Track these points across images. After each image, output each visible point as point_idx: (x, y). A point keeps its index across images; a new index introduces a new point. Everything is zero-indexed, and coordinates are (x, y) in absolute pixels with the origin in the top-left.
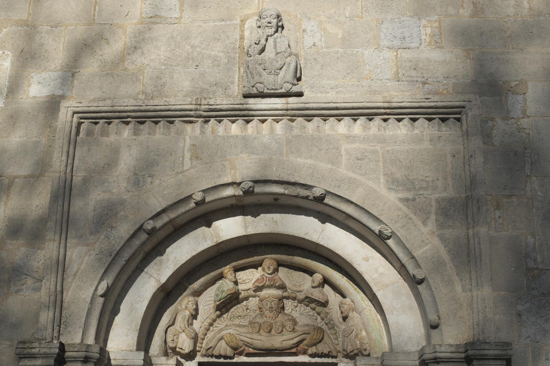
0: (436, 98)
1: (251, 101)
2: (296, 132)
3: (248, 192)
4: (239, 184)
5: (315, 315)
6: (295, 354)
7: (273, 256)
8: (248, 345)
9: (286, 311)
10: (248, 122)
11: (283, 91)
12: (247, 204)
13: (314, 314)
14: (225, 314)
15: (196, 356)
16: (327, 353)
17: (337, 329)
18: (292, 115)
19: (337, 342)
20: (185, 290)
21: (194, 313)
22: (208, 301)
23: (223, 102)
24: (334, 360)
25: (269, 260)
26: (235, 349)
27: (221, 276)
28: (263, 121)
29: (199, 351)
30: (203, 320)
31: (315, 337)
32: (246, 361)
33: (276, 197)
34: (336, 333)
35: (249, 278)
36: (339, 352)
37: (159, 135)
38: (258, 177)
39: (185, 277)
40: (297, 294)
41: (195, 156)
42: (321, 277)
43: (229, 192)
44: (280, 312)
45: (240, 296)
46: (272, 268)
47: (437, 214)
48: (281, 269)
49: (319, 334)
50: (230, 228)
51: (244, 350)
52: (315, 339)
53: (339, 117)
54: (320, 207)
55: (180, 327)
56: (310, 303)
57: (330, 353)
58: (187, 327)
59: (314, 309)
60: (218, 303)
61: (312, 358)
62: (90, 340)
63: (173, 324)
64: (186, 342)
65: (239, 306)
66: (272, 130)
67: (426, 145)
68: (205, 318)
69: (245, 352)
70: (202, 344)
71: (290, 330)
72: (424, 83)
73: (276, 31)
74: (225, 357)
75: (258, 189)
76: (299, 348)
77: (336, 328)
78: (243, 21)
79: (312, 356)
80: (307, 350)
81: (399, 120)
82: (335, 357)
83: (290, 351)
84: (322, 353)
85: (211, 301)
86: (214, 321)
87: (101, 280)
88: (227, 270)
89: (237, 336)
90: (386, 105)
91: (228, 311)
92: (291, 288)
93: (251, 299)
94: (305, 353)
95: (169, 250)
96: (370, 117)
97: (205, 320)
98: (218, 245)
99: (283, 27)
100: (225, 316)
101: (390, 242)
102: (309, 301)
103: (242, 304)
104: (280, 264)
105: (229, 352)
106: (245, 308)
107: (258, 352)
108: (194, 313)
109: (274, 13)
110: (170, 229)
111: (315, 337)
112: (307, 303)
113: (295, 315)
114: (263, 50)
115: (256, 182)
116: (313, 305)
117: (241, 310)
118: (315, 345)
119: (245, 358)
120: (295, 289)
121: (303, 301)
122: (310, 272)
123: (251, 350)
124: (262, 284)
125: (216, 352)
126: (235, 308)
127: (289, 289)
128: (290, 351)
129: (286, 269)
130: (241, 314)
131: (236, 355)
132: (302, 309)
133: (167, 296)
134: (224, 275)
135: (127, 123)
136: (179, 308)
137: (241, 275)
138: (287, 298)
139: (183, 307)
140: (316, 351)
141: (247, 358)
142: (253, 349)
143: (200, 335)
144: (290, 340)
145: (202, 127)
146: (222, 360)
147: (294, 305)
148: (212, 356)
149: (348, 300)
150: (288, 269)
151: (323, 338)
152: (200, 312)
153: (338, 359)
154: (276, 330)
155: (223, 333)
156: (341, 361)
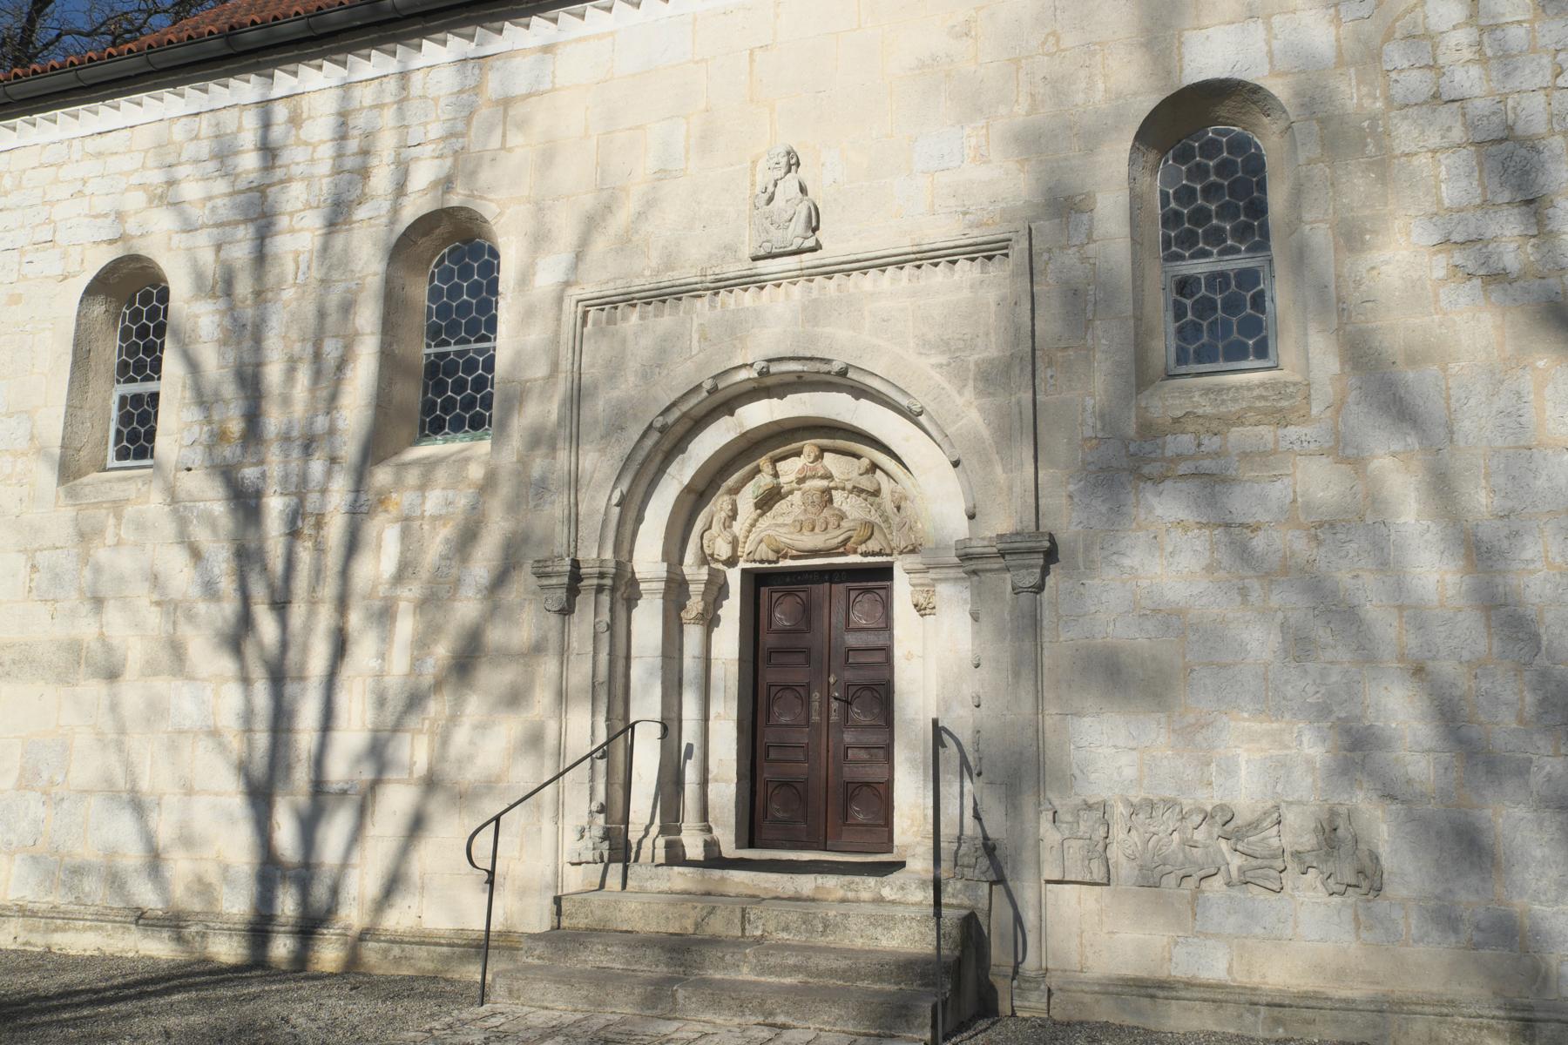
0: (975, 232)
1: (760, 263)
2: (815, 294)
3: (763, 373)
4: (751, 365)
10: (762, 288)
11: (793, 248)
12: (767, 386)
18: (810, 275)
22: (747, 500)
23: (732, 270)
24: (889, 559)
25: (809, 446)
26: (777, 552)
27: (758, 471)
28: (779, 286)
33: (799, 375)
35: (790, 469)
37: (665, 320)
38: (772, 356)
41: (704, 338)
43: (743, 375)
47: (975, 380)
50: (758, 414)
53: (864, 270)
54: (840, 381)
62: (608, 554)
63: (710, 527)
66: (787, 295)
67: (966, 293)
72: (965, 213)
73: (789, 171)
75: (774, 368)
78: (754, 163)
79: (865, 554)
81: (936, 265)
87: (614, 487)
88: (764, 462)
90: (915, 249)
91: (771, 508)
94: (855, 552)
95: (691, 447)
96: (900, 265)
98: (743, 435)
99: (798, 164)
101: (922, 419)
105: (772, 556)
109: (783, 150)
110: (688, 423)
113: (845, 508)
114: (771, 199)
115: (770, 361)
122: (858, 457)
133: (698, 495)
135: (634, 306)
137: (781, 466)
138: (836, 488)
143: (741, 539)
145: (711, 301)
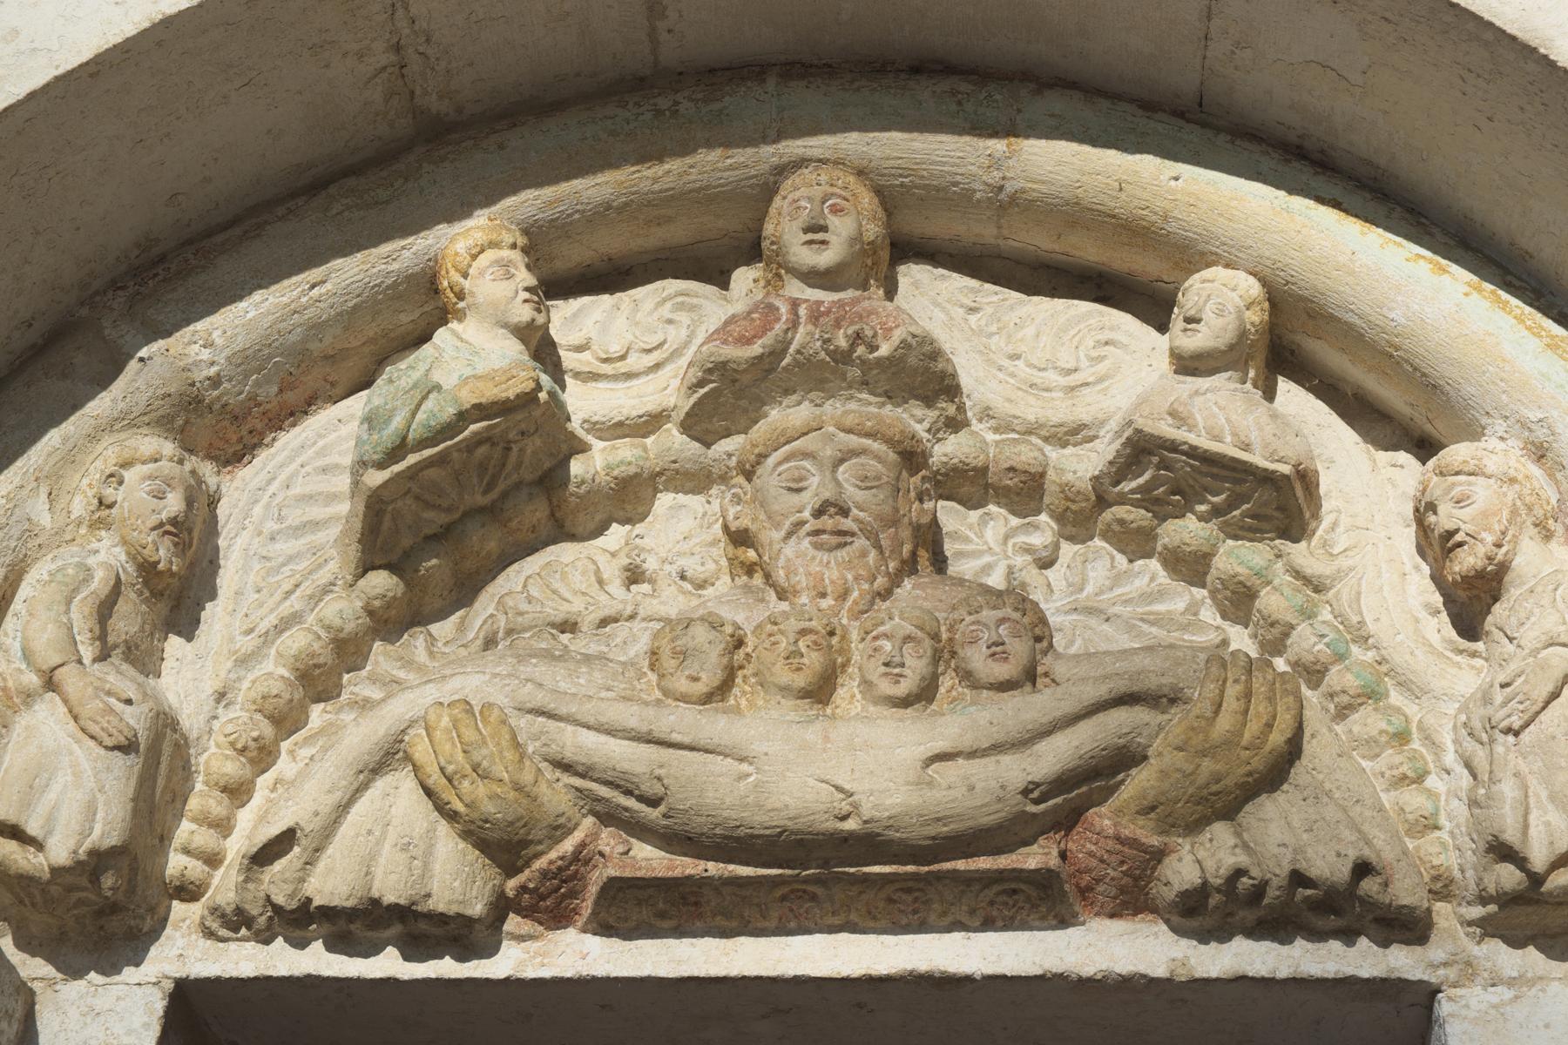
5: (1209, 615)
6: (1043, 901)
7: (852, 143)
8: (624, 806)
9: (952, 570)
13: (1193, 609)
14: (442, 615)
16: (1343, 872)
17: (1412, 709)
19: (1413, 800)
21: (164, 554)
22: (296, 502)
24: (1401, 961)
26: (502, 845)
29: (188, 891)
30: (247, 644)
31: (1224, 723)
32: (600, 970)
34: (1402, 737)
36: (1443, 888)
39: (115, 285)
40: (1053, 453)
42: (1253, 288)
44: (909, 567)
45: (577, 467)
46: (841, 229)
48: (912, 276)
49: (1259, 707)
51: (581, 858)
52: (1231, 741)
55: (27, 655)
56: (1161, 506)
57: (1369, 886)
58: (87, 653)
59: (1190, 566)
60: (375, 478)
61: (1204, 936)
65: (565, 552)
68: (272, 619)
69: (596, 879)
70: (223, 826)
71: (1002, 671)
74: (419, 928)
76: (1081, 844)
77: (1395, 698)
79: (1202, 913)
80: (1159, 855)
82: (1407, 927)
83: (1003, 862)
84: (1298, 878)
85: (332, 498)
86: (348, 651)
89: (522, 723)
91: (465, 590)
92: (1001, 406)
93: (665, 500)
94: (1133, 898)
97: (267, 638)
100: (442, 629)
102: (1162, 479)
103: (600, 542)
104: (909, 236)
105: (453, 878)
106: (612, 571)
107: (714, 868)
108: (164, 554)
111: (1224, 723)
112: (1137, 516)
116: (1188, 530)
117: (578, 580)
118: (1226, 803)
119: (594, 943)
120: (1031, 410)
121: (1102, 502)
123: (649, 859)
124: (756, 349)
125: (330, 883)
126: (532, 564)
127: (986, 414)
128: (1003, 862)
129: (957, 283)
130: (577, 605)
131: (513, 923)
132: (1098, 574)
134: (449, 277)
136: (45, 520)
139: (80, 506)
140: (1242, 859)
141: (616, 943)
142: (676, 840)
143: (214, 760)
144: (997, 748)
146: (388, 964)
147: (1028, 549)
148: (298, 921)
149: (1496, 452)
150: (974, 283)
151: (1293, 750)
153: (1436, 951)
154: (875, 671)
155: (400, 708)
156: (1469, 970)
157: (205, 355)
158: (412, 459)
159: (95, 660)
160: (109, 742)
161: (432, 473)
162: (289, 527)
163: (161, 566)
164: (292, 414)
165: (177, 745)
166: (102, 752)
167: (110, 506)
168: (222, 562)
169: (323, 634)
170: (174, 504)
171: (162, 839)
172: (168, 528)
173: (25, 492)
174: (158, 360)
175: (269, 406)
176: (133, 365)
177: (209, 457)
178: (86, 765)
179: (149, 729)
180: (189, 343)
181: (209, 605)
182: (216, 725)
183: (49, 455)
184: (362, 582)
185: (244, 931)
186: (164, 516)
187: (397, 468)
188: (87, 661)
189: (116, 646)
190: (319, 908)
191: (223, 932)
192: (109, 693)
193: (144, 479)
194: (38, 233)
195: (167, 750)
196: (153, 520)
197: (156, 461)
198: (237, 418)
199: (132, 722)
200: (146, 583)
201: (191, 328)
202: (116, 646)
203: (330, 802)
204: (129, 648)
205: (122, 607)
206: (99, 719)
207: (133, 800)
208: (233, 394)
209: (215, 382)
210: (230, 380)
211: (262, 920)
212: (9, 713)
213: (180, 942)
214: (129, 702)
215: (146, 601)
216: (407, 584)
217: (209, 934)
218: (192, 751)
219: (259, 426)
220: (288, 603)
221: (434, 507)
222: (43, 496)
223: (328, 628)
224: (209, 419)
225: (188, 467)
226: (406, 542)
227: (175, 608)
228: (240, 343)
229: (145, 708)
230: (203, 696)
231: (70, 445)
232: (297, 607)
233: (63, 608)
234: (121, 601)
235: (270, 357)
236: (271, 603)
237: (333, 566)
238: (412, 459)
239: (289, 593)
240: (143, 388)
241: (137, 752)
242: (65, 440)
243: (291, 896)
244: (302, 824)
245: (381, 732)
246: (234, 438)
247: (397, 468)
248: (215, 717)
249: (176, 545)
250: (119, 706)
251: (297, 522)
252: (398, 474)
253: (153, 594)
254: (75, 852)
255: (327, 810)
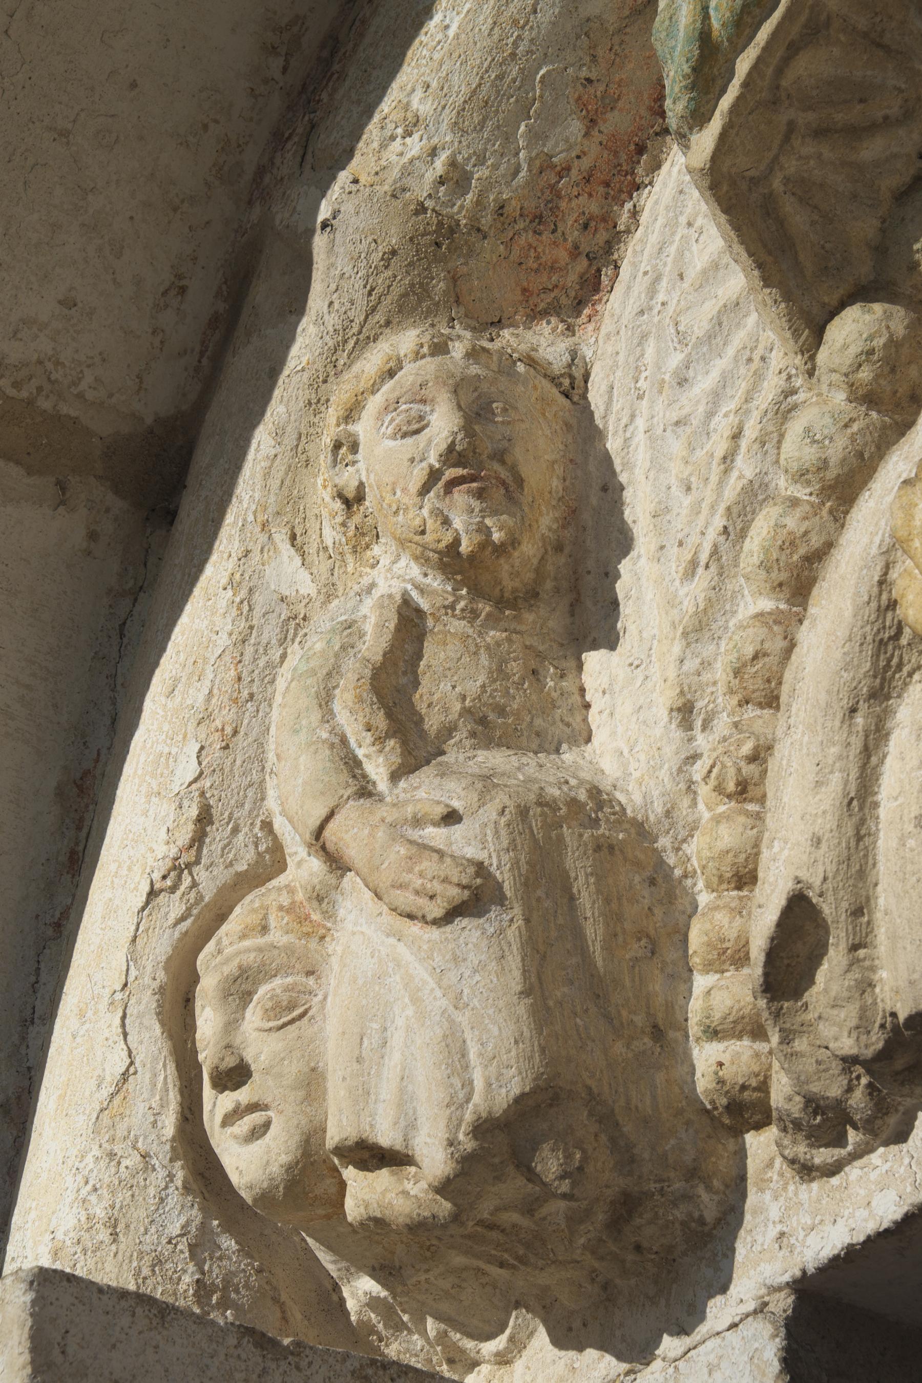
15: (731, 1215)
20: (295, 304)
21: (463, 518)
30: (694, 593)
64: (403, 1015)
152: (638, 508)
157: (415, 145)
158: (743, 65)
159: (395, 777)
160: (436, 910)
161: (809, 67)
162: (700, 342)
163: (465, 547)
164: (641, 149)
165: (604, 849)
166: (435, 933)
167: (360, 498)
168: (623, 478)
169: (801, 492)
170: (443, 424)
171: (657, 1033)
172: (451, 473)
173: (256, 557)
174: (348, 208)
175: (586, 163)
176: (320, 242)
177: (535, 315)
178: (421, 972)
179: (513, 846)
180: (383, 146)
181: (624, 567)
182: (698, 770)
183: (267, 475)
184: (822, 356)
185: (853, 1136)
186: (433, 459)
187: (726, 102)
188: (381, 782)
189: (449, 730)
190: (911, 1019)
191: (823, 1156)
192: (418, 822)
193: (379, 418)
194: (65, 134)
195: (578, 866)
196: (419, 474)
197: (391, 373)
198: (539, 218)
199: (471, 852)
200: (477, 592)
201: (376, 118)
202: (449, 730)
203: (827, 805)
204: (483, 721)
205: (435, 655)
206: (406, 877)
207: (526, 992)
208: (504, 178)
209: (456, 178)
210: (481, 160)
211: (858, 1100)
212: (313, 944)
213: (774, 1211)
214: (451, 818)
215: (493, 621)
216: (911, 303)
217: (807, 1171)
218: (664, 842)
219: (594, 207)
220: (735, 474)
221: (872, 128)
222: (285, 547)
223: (801, 476)
224: (490, 249)
225: (458, 350)
226: (864, 227)
227: (574, 607)
228: (461, 86)
229: (490, 812)
230: (658, 731)
231: (290, 440)
232: (749, 474)
233: (316, 716)
234: (429, 647)
235: (527, 76)
236: (709, 495)
237: (777, 360)
238: (743, 65)
239: (728, 459)
240: (348, 270)
241: (500, 899)
242: (278, 434)
243: (862, 1027)
244: (803, 874)
245: (848, 613)
246: (562, 255)
247: (726, 102)
248: (693, 758)
249: (480, 494)
250: (434, 835)
251: (706, 325)
252: (734, 109)
253: (501, 603)
254: (451, 1143)
255: (830, 822)
